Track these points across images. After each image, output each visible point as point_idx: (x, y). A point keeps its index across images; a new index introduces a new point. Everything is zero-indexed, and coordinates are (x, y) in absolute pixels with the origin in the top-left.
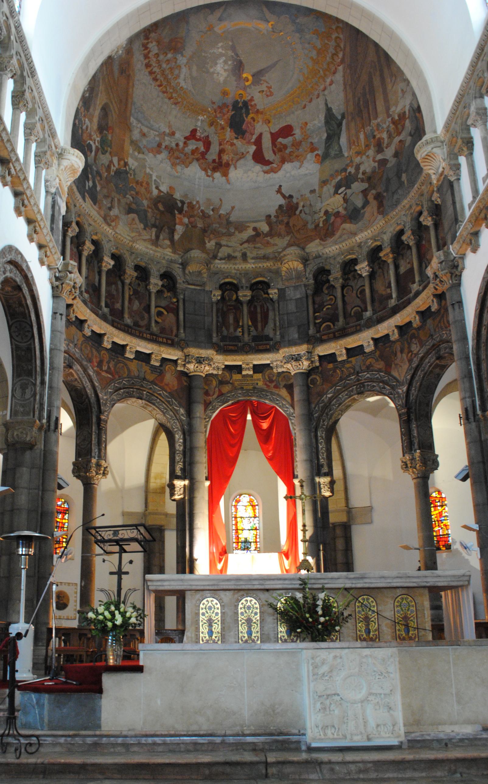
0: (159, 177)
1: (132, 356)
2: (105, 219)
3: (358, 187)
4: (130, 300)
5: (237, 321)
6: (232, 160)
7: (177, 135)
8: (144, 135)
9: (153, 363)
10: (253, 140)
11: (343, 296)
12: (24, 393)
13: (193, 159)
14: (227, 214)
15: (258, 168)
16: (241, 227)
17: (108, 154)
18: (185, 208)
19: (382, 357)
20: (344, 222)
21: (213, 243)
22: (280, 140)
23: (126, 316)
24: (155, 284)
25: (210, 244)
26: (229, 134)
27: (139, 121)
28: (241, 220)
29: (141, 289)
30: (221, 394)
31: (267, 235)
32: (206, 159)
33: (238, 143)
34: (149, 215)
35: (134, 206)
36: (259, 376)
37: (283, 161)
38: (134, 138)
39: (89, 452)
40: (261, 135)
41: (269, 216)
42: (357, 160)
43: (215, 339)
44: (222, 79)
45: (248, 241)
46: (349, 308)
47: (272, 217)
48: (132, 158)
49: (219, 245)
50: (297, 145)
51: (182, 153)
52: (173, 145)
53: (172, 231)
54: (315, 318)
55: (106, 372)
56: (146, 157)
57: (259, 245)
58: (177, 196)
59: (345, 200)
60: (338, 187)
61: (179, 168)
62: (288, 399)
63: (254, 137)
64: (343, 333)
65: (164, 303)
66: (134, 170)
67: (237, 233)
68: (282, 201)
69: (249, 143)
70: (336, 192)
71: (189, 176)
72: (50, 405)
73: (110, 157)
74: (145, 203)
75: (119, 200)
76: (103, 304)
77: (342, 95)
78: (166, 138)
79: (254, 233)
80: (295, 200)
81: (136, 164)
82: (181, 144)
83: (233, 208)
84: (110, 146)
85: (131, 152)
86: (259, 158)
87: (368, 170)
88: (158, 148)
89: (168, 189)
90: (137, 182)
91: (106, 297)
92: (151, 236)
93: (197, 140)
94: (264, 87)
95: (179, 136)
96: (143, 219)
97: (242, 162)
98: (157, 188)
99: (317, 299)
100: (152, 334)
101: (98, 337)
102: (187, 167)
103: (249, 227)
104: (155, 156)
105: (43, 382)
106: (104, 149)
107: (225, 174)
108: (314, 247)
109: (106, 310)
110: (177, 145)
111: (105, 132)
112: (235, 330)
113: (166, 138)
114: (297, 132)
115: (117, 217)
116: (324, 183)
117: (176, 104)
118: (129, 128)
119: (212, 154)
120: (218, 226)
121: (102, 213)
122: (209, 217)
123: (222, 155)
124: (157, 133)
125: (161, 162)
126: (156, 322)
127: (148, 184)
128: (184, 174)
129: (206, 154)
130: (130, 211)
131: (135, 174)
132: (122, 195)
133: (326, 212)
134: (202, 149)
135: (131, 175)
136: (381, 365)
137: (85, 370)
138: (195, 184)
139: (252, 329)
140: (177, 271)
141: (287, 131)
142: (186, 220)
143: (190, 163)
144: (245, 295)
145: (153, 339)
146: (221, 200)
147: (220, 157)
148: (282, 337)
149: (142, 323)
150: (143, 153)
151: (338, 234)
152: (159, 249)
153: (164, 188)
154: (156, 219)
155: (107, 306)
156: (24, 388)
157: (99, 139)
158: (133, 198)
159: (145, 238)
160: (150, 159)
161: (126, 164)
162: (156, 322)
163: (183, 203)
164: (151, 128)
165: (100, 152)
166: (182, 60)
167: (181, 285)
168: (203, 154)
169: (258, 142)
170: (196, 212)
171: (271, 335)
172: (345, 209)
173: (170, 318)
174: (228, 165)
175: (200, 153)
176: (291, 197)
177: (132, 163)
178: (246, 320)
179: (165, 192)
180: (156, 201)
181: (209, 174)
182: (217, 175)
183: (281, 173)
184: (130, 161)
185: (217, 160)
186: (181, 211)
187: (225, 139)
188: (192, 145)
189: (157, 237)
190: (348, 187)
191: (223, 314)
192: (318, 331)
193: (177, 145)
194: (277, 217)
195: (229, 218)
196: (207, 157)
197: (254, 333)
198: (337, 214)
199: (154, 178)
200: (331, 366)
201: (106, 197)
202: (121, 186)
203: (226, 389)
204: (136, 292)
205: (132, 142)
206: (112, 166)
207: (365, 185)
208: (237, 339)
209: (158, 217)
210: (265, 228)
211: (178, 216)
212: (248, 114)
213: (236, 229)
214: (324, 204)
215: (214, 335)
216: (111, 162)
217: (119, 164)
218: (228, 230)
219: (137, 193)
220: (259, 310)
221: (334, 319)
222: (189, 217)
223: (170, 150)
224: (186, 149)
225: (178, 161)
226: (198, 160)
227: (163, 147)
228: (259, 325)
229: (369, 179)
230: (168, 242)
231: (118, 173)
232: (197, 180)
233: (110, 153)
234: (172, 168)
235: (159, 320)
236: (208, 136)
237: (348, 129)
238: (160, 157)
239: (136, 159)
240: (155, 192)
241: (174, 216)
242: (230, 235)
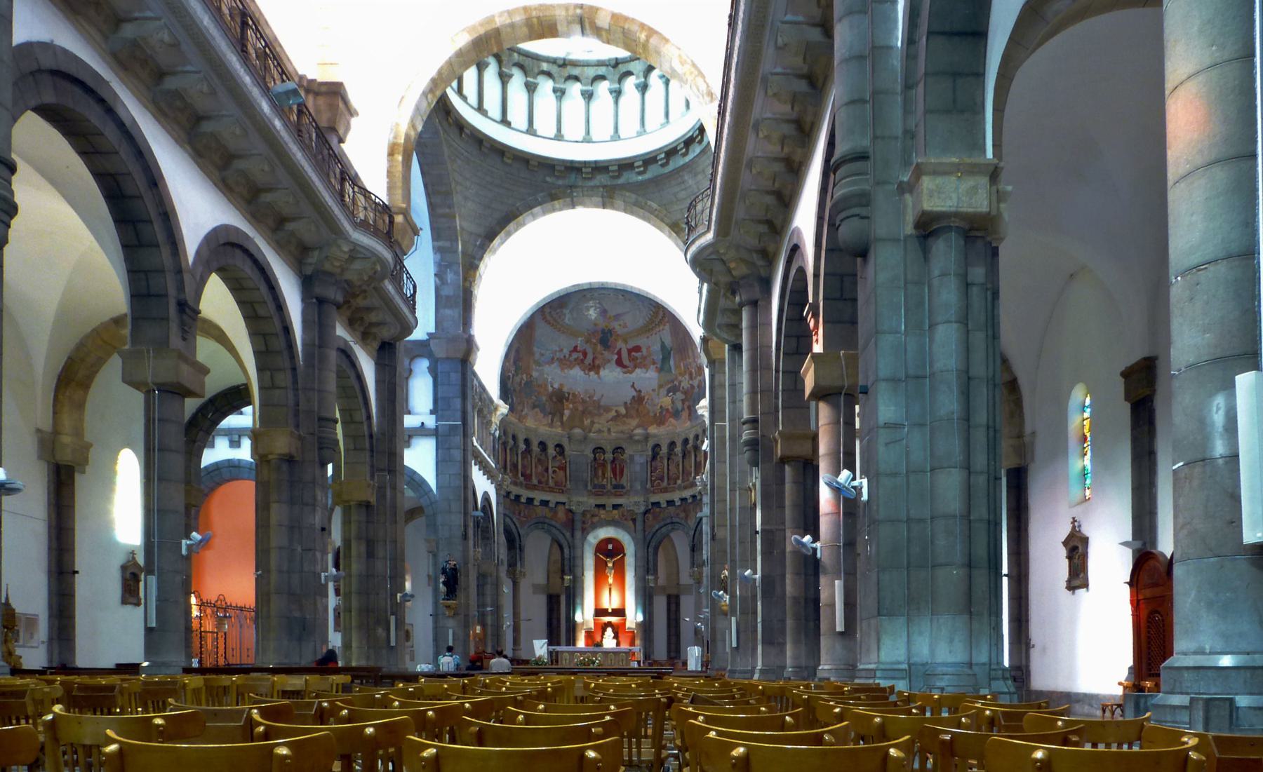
0: (552, 379)
1: (538, 504)
2: (519, 420)
3: (679, 396)
4: (536, 467)
5: (604, 474)
7: (565, 351)
8: (542, 355)
11: (668, 465)
15: (619, 369)
16: (607, 410)
18: (571, 397)
19: (684, 511)
20: (671, 417)
21: (589, 421)
22: (633, 353)
23: (533, 478)
24: (551, 451)
25: (587, 422)
26: (599, 347)
29: (543, 458)
30: (592, 523)
31: (624, 416)
33: (606, 353)
34: (547, 407)
37: (635, 367)
38: (536, 359)
39: (515, 565)
41: (626, 403)
42: (680, 378)
43: (589, 488)
44: (593, 318)
45: (611, 420)
46: (671, 473)
49: (593, 423)
50: (644, 358)
52: (562, 357)
53: (562, 415)
54: (652, 476)
58: (565, 389)
59: (673, 402)
60: (669, 391)
61: (566, 371)
62: (633, 526)
64: (665, 490)
65: (557, 464)
68: (634, 394)
69: (613, 353)
70: (667, 395)
72: (498, 553)
76: (520, 475)
77: (670, 338)
79: (615, 414)
80: (642, 394)
82: (567, 356)
83: (602, 396)
86: (619, 363)
87: (685, 387)
88: (552, 361)
94: (621, 322)
95: (566, 351)
96: (543, 410)
98: (552, 386)
99: (653, 463)
107: (598, 373)
108: (653, 430)
109: (522, 479)
110: (565, 357)
114: (644, 350)
116: (661, 386)
117: (563, 333)
119: (589, 360)
127: (546, 385)
130: (534, 407)
133: (661, 407)
134: (582, 357)
136: (682, 515)
137: (512, 520)
139: (613, 480)
140: (565, 443)
141: (637, 349)
143: (574, 366)
144: (609, 456)
145: (551, 490)
147: (593, 361)
148: (631, 487)
149: (543, 480)
151: (667, 424)
152: (554, 430)
153: (556, 386)
155: (522, 475)
160: (547, 368)
161: (531, 376)
166: (566, 311)
168: (582, 361)
169: (619, 353)
171: (625, 484)
172: (672, 408)
173: (561, 473)
174: (599, 367)
176: (640, 391)
177: (535, 374)
178: (609, 474)
180: (550, 396)
182: (592, 373)
183: (634, 375)
186: (567, 399)
188: (575, 355)
190: (674, 394)
191: (595, 470)
192: (653, 486)
193: (565, 357)
197: (614, 482)
198: (667, 410)
200: (658, 510)
201: (519, 404)
203: (595, 519)
207: (683, 397)
208: (603, 487)
210: (623, 411)
212: (611, 336)
214: (661, 400)
215: (589, 484)
216: (522, 379)
220: (618, 466)
221: (662, 479)
222: (573, 403)
223: (560, 360)
226: (578, 364)
229: (685, 393)
236: (585, 350)
237: (674, 358)
238: (553, 366)
240: (550, 389)
242: (600, 415)
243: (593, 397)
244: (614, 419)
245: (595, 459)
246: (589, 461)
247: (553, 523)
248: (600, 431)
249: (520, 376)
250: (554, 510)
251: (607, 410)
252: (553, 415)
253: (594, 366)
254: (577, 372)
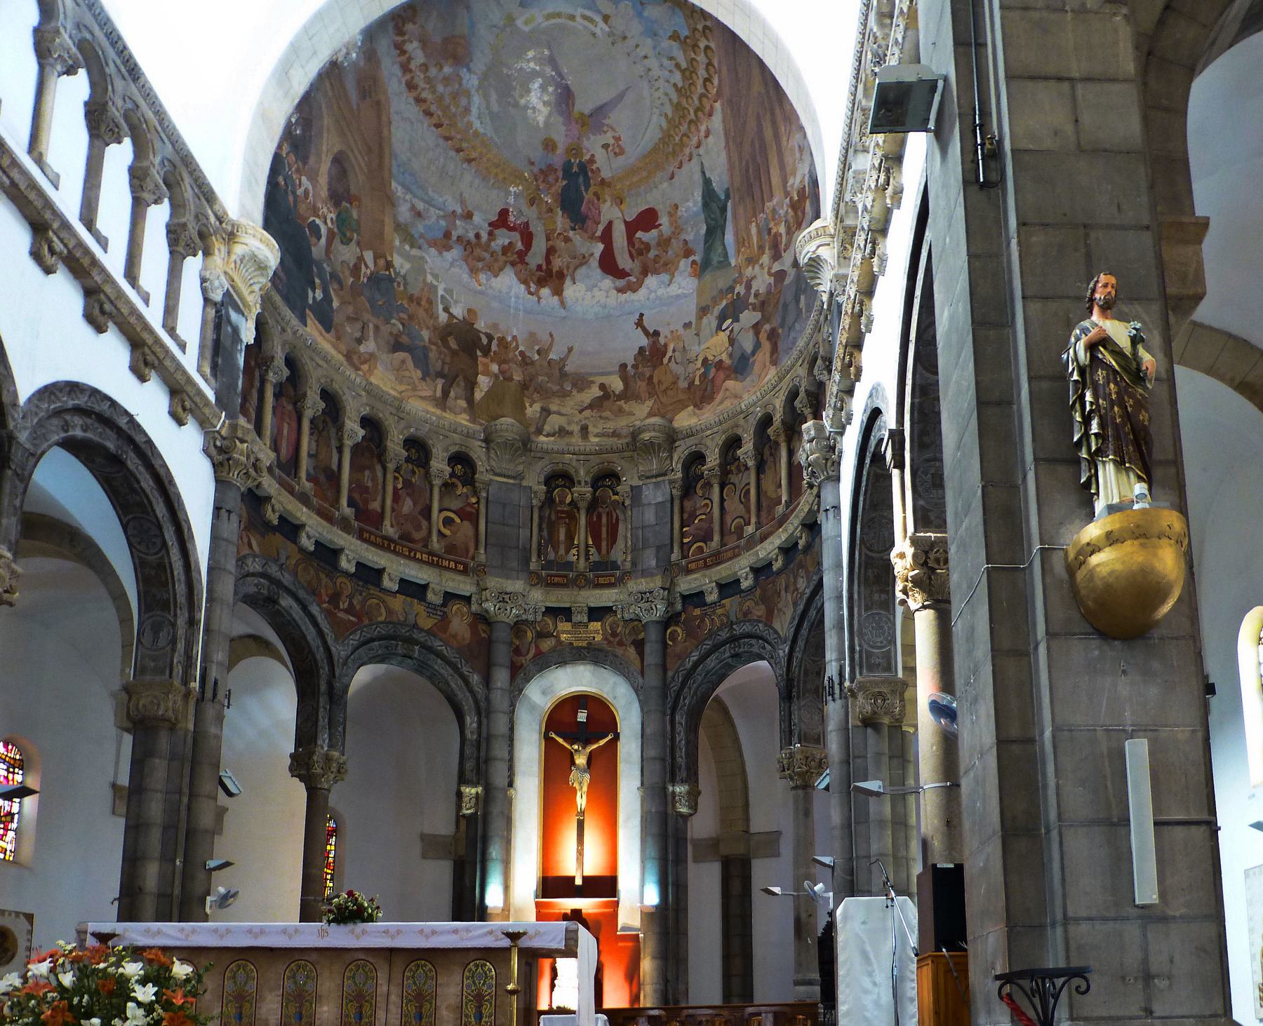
6: (568, 268)
7: (477, 218)
8: (419, 214)
13: (506, 262)
14: (561, 360)
16: (581, 382)
17: (353, 244)
18: (494, 347)
27: (407, 189)
28: (582, 371)
32: (527, 264)
34: (433, 355)
35: (405, 339)
38: (402, 220)
41: (623, 366)
47: (629, 368)
48: (401, 255)
51: (486, 251)
52: (471, 235)
53: (471, 385)
56: (424, 254)
58: (481, 325)
61: (482, 277)
66: (404, 277)
67: (575, 392)
71: (500, 292)
73: (358, 250)
74: (426, 334)
75: (377, 328)
78: (458, 222)
81: (407, 266)
82: (484, 236)
83: (570, 350)
84: (358, 231)
85: (397, 243)
89: (466, 312)
90: (411, 298)
92: (435, 391)
93: (511, 229)
95: (481, 221)
97: (582, 271)
98: (446, 310)
102: (496, 276)
103: (593, 382)
104: (441, 253)
106: (345, 236)
107: (558, 292)
110: (478, 236)
111: (344, 204)
113: (458, 222)
118: (390, 201)
119: (536, 256)
120: (546, 379)
122: (533, 363)
123: (551, 257)
124: (441, 213)
125: (452, 264)
127: (430, 302)
128: (491, 287)
129: (526, 255)
130: (397, 346)
131: (405, 285)
132: (382, 318)
134: (519, 246)
135: (399, 286)
138: (510, 307)
142: (495, 368)
143: (501, 269)
146: (551, 335)
147: (548, 261)
150: (420, 248)
154: (444, 363)
157: (333, 216)
158: (403, 324)
159: (424, 394)
160: (433, 259)
161: (389, 265)
164: (430, 203)
165: (337, 241)
168: (522, 255)
170: (511, 355)
174: (561, 276)
175: (517, 253)
179: (461, 317)
181: (532, 290)
182: (545, 292)
184: (397, 261)
185: (544, 267)
186: (486, 351)
187: (555, 230)
188: (503, 238)
189: (446, 394)
193: (478, 236)
194: (635, 367)
195: (564, 365)
196: (527, 259)
199: (441, 292)
202: (380, 303)
205: (399, 227)
206: (363, 266)
209: (448, 360)
211: (481, 359)
213: (574, 385)
216: (361, 259)
217: (376, 264)
218: (562, 386)
219: (411, 317)
224: (492, 244)
225: (480, 265)
226: (513, 264)
227: (454, 238)
232: (513, 299)
233: (358, 244)
234: (471, 277)
236: (527, 224)
238: (449, 256)
239: (408, 257)
240: (443, 317)
241: (475, 359)
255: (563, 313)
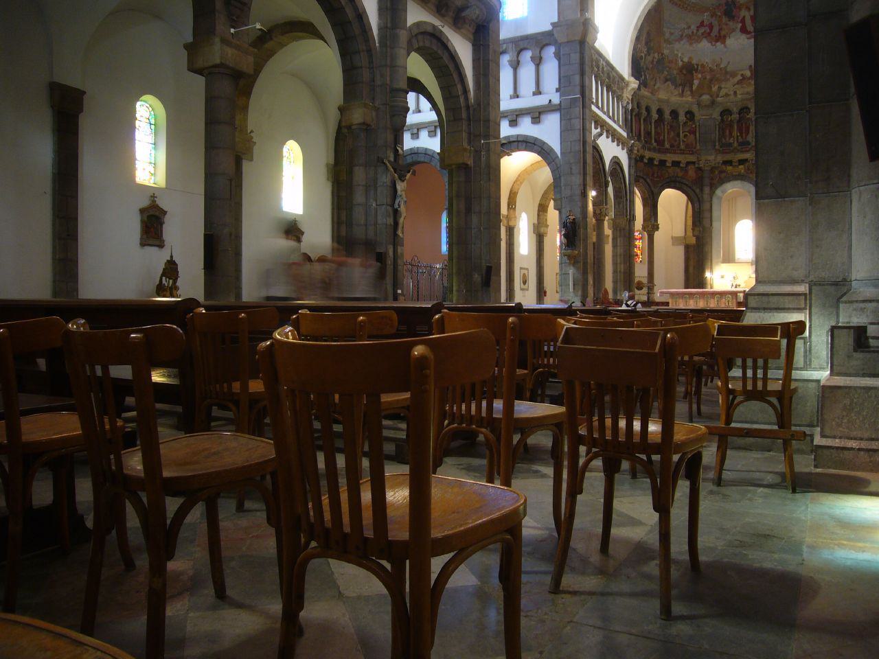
0: (682, 54)
2: (652, 93)
5: (731, 134)
7: (693, 27)
8: (672, 34)
9: (681, 165)
10: (739, 21)
12: (619, 207)
15: (744, 36)
16: (733, 75)
18: (699, 68)
21: (717, 87)
24: (682, 118)
25: (715, 89)
26: (724, 19)
33: (731, 23)
34: (678, 79)
35: (668, 77)
36: (741, 167)
40: (744, 17)
43: (717, 147)
45: (738, 83)
49: (720, 88)
52: (690, 33)
53: (691, 87)
55: (656, 178)
57: (745, 85)
58: (694, 62)
61: (694, 45)
63: (740, 18)
76: (653, 141)
79: (741, 78)
81: (668, 51)
82: (695, 31)
83: (729, 63)
91: (655, 135)
97: (734, 33)
100: (681, 150)
101: (651, 160)
105: (627, 200)
107: (724, 43)
110: (693, 32)
112: (730, 139)
115: (659, 88)
121: (650, 90)
126: (683, 141)
127: (676, 60)
130: (667, 80)
134: (708, 30)
139: (740, 137)
140: (695, 109)
142: (700, 76)
143: (701, 41)
144: (735, 116)
146: (721, 59)
147: (719, 32)
152: (684, 99)
153: (686, 60)
155: (656, 141)
156: (619, 204)
160: (677, 45)
162: (683, 141)
163: (697, 65)
167: (697, 117)
168: (709, 34)
169: (743, 21)
171: (751, 141)
173: (692, 136)
174: (725, 37)
177: (666, 52)
178: (735, 133)
180: (681, 70)
182: (718, 44)
186: (696, 70)
188: (702, 30)
193: (693, 32)
196: (712, 34)
197: (740, 140)
199: (680, 55)
201: (652, 79)
204: (671, 126)
208: (730, 145)
213: (731, 76)
215: (717, 144)
216: (654, 57)
226: (706, 37)
228: (744, 135)
230: (689, 93)
231: (659, 61)
235: (685, 140)
238: (682, 42)
243: (719, 65)
244: (739, 82)
245: (722, 120)
246: (717, 123)
247: (684, 181)
248: (727, 95)
249: (652, 55)
250: (685, 170)
251: (733, 75)
252: (683, 85)
253: (720, 36)
254: (705, 44)
255: (726, 49)
